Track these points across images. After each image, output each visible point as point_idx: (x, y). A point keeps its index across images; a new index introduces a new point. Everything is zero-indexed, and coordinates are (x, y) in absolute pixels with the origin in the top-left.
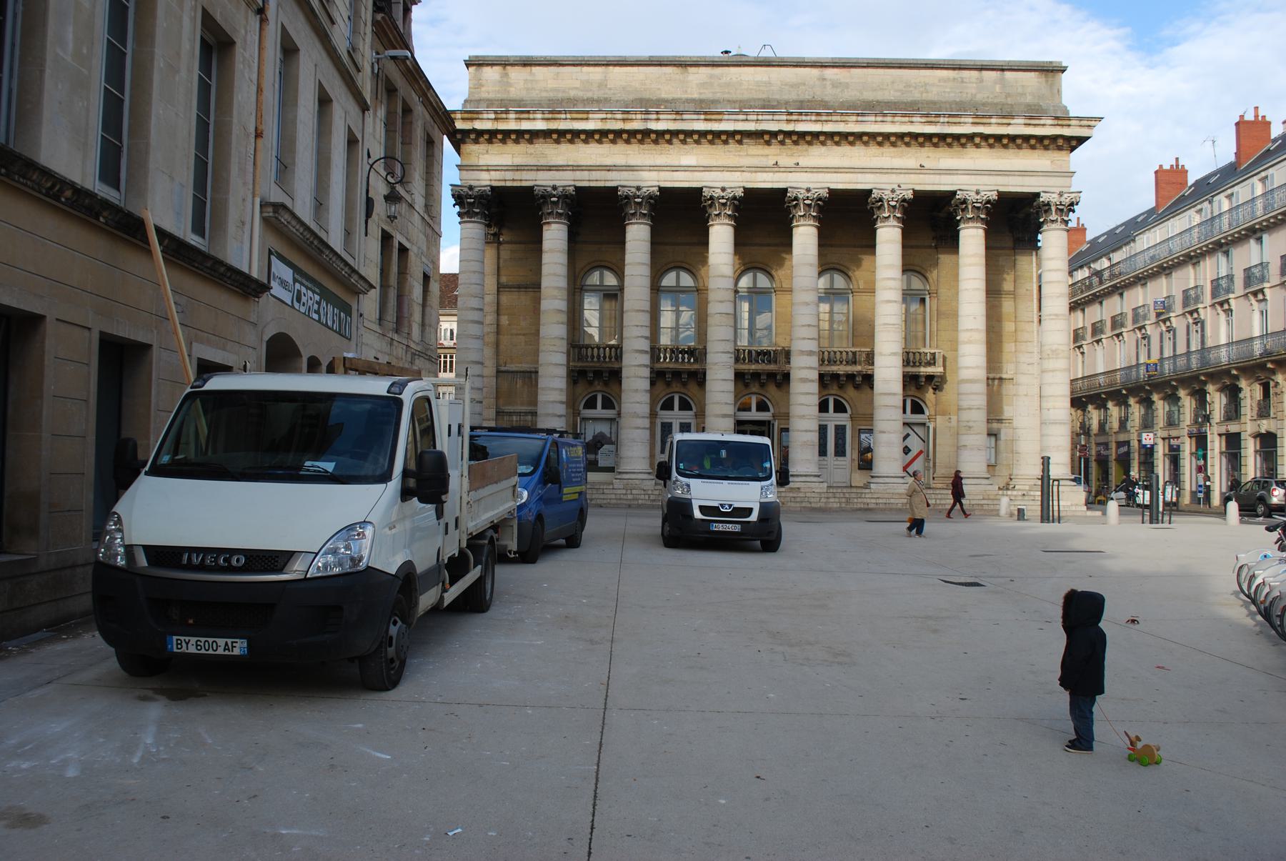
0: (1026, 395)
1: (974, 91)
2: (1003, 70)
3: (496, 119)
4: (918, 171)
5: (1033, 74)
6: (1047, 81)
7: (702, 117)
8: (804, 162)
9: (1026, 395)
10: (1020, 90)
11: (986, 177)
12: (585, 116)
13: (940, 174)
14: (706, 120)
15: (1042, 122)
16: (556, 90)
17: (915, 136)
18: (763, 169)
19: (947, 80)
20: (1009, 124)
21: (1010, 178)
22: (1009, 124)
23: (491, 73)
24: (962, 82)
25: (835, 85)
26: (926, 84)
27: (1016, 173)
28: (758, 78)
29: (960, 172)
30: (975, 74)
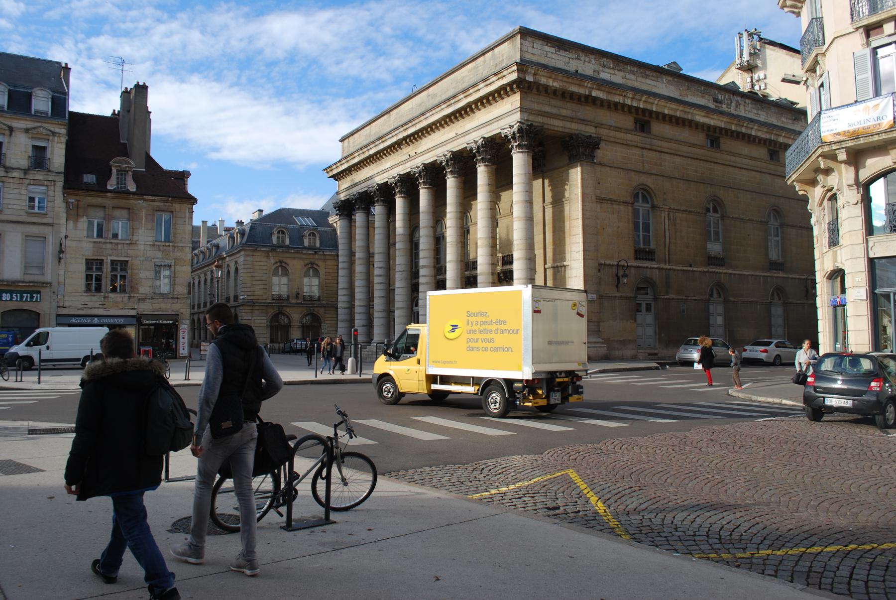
0: (576, 277)
1: (481, 71)
2: (493, 49)
3: (337, 167)
4: (456, 138)
5: (506, 44)
6: (513, 45)
7: (381, 141)
8: (419, 150)
9: (576, 277)
10: (501, 59)
11: (482, 129)
12: (352, 157)
13: (464, 136)
14: (383, 142)
15: (491, 80)
16: (360, 144)
17: (449, 116)
18: (406, 161)
19: (470, 71)
20: (479, 90)
21: (493, 125)
22: (479, 90)
23: (346, 142)
24: (478, 67)
25: (434, 96)
26: (463, 77)
27: (494, 120)
28: (410, 106)
29: (471, 131)
30: (482, 58)
